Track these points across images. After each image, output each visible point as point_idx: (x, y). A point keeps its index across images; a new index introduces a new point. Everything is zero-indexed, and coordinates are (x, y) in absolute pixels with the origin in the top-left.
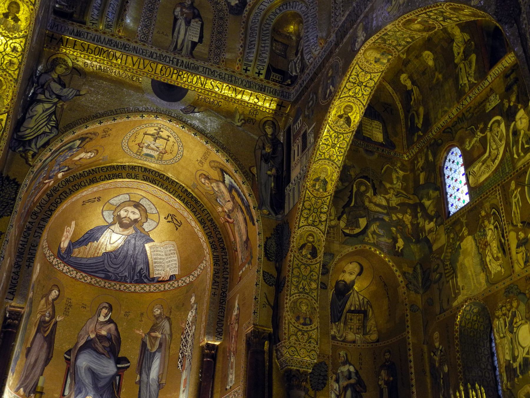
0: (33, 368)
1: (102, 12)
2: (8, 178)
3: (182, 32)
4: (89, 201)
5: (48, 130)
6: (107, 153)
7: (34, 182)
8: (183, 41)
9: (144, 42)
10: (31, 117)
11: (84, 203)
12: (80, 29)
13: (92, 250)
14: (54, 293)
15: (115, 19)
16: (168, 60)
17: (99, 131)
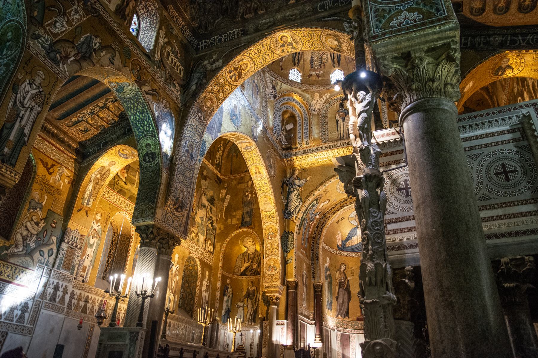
0: (342, 305)
1: (301, 138)
2: (289, 232)
3: (342, 126)
4: (339, 221)
5: (298, 204)
6: (334, 198)
7: (302, 228)
8: (344, 131)
9: (325, 143)
10: (291, 201)
11: (337, 223)
12: (297, 151)
13: (356, 240)
14: (343, 267)
15: (309, 139)
16: (338, 145)
17: (322, 193)
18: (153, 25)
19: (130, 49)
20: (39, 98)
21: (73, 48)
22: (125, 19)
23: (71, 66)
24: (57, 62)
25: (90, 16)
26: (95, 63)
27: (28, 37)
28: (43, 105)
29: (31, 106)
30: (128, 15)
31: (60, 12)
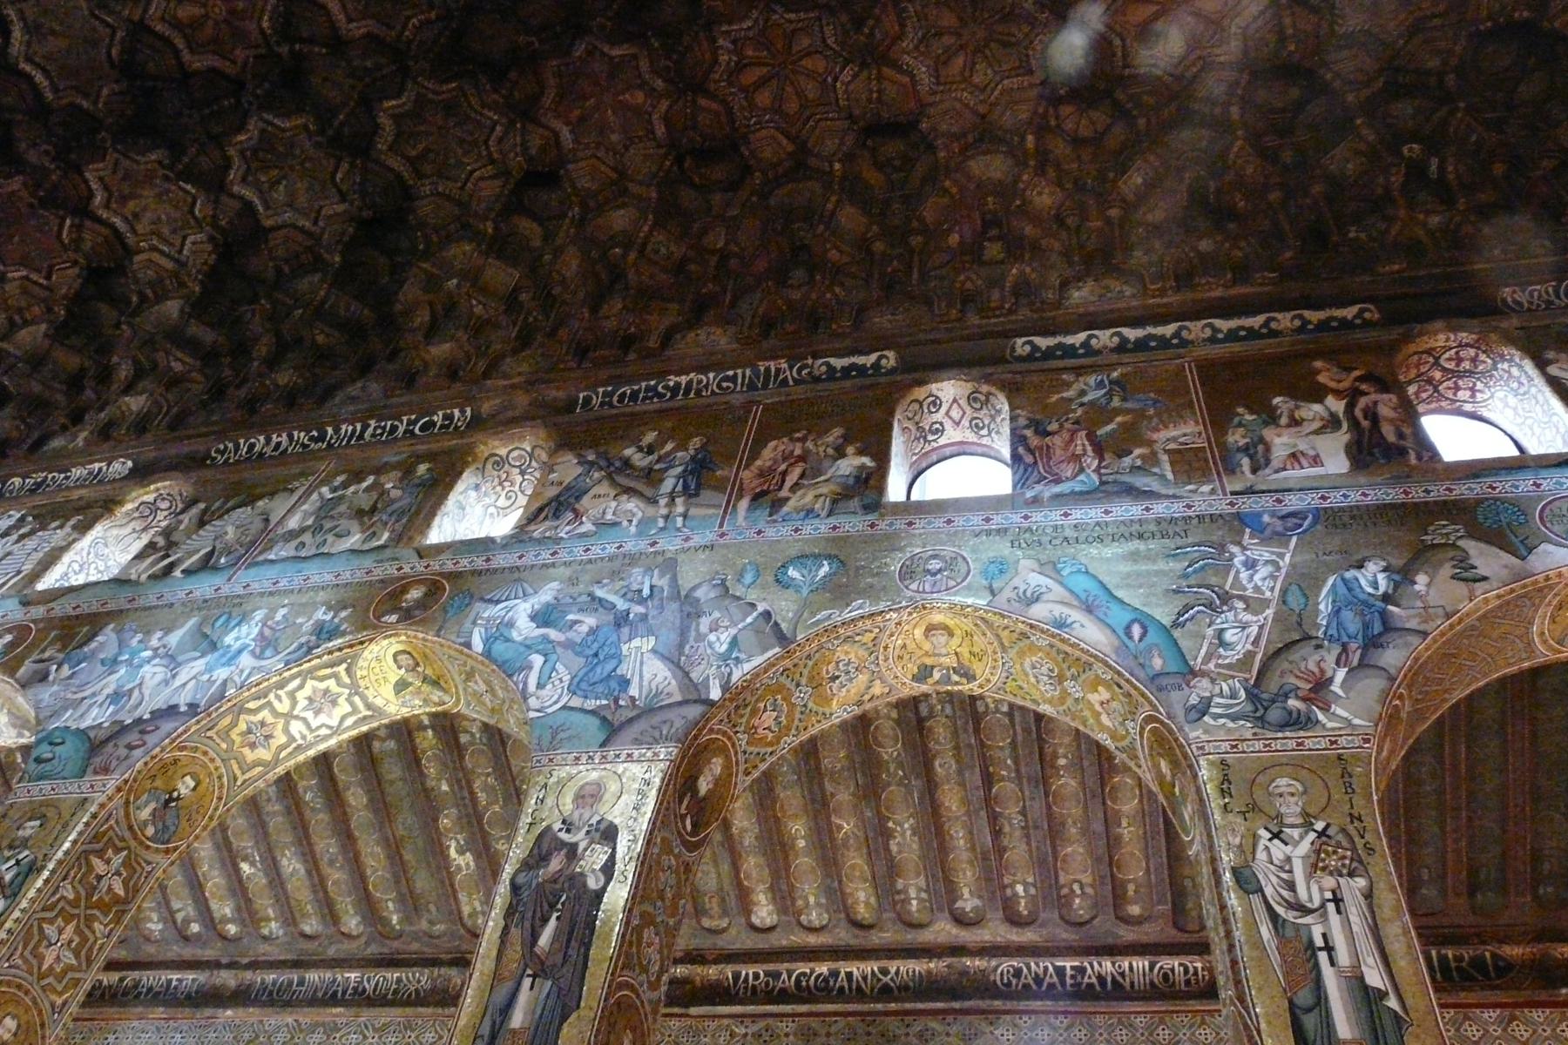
18: (1521, 384)
19: (1496, 499)
20: (1335, 852)
21: (1318, 647)
22: (1403, 452)
23: (1352, 694)
24: (1303, 719)
25: (1294, 539)
26: (1422, 628)
27: (1181, 729)
28: (1361, 862)
29: (1329, 895)
30: (1401, 436)
31: (1210, 605)
